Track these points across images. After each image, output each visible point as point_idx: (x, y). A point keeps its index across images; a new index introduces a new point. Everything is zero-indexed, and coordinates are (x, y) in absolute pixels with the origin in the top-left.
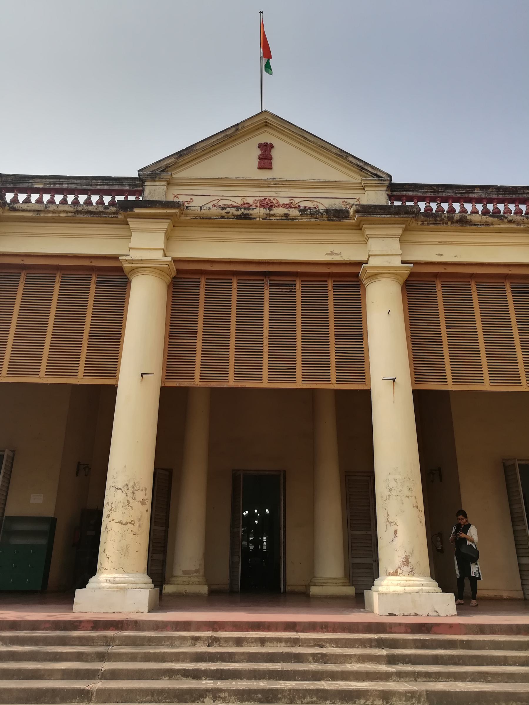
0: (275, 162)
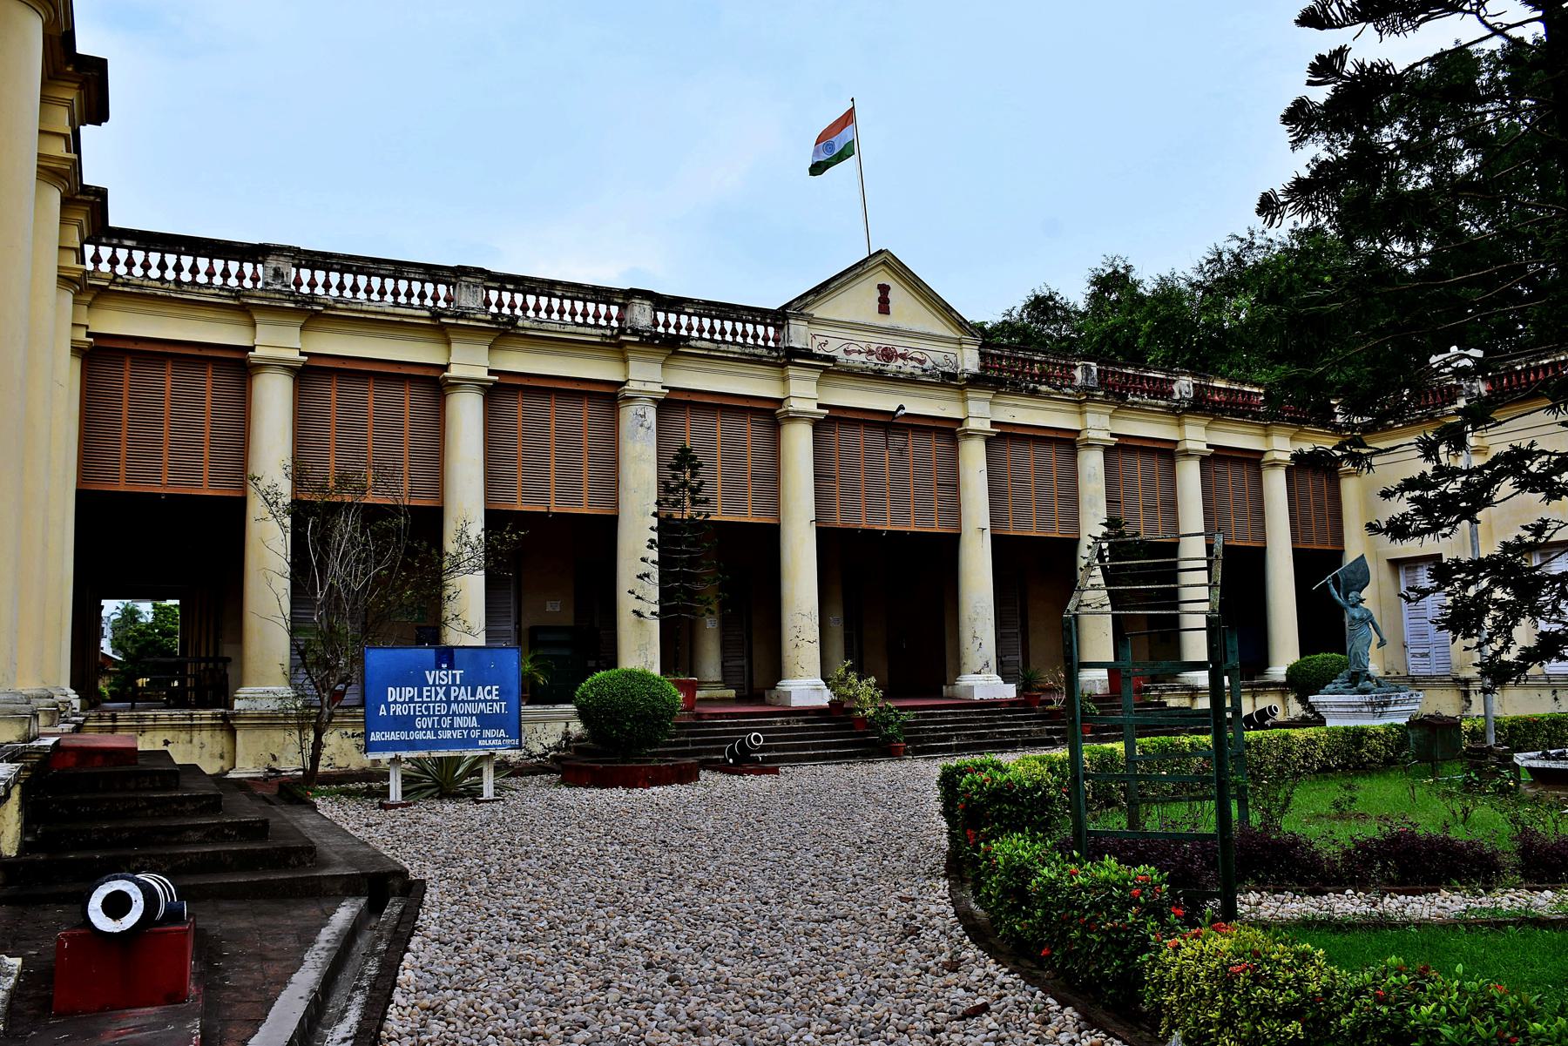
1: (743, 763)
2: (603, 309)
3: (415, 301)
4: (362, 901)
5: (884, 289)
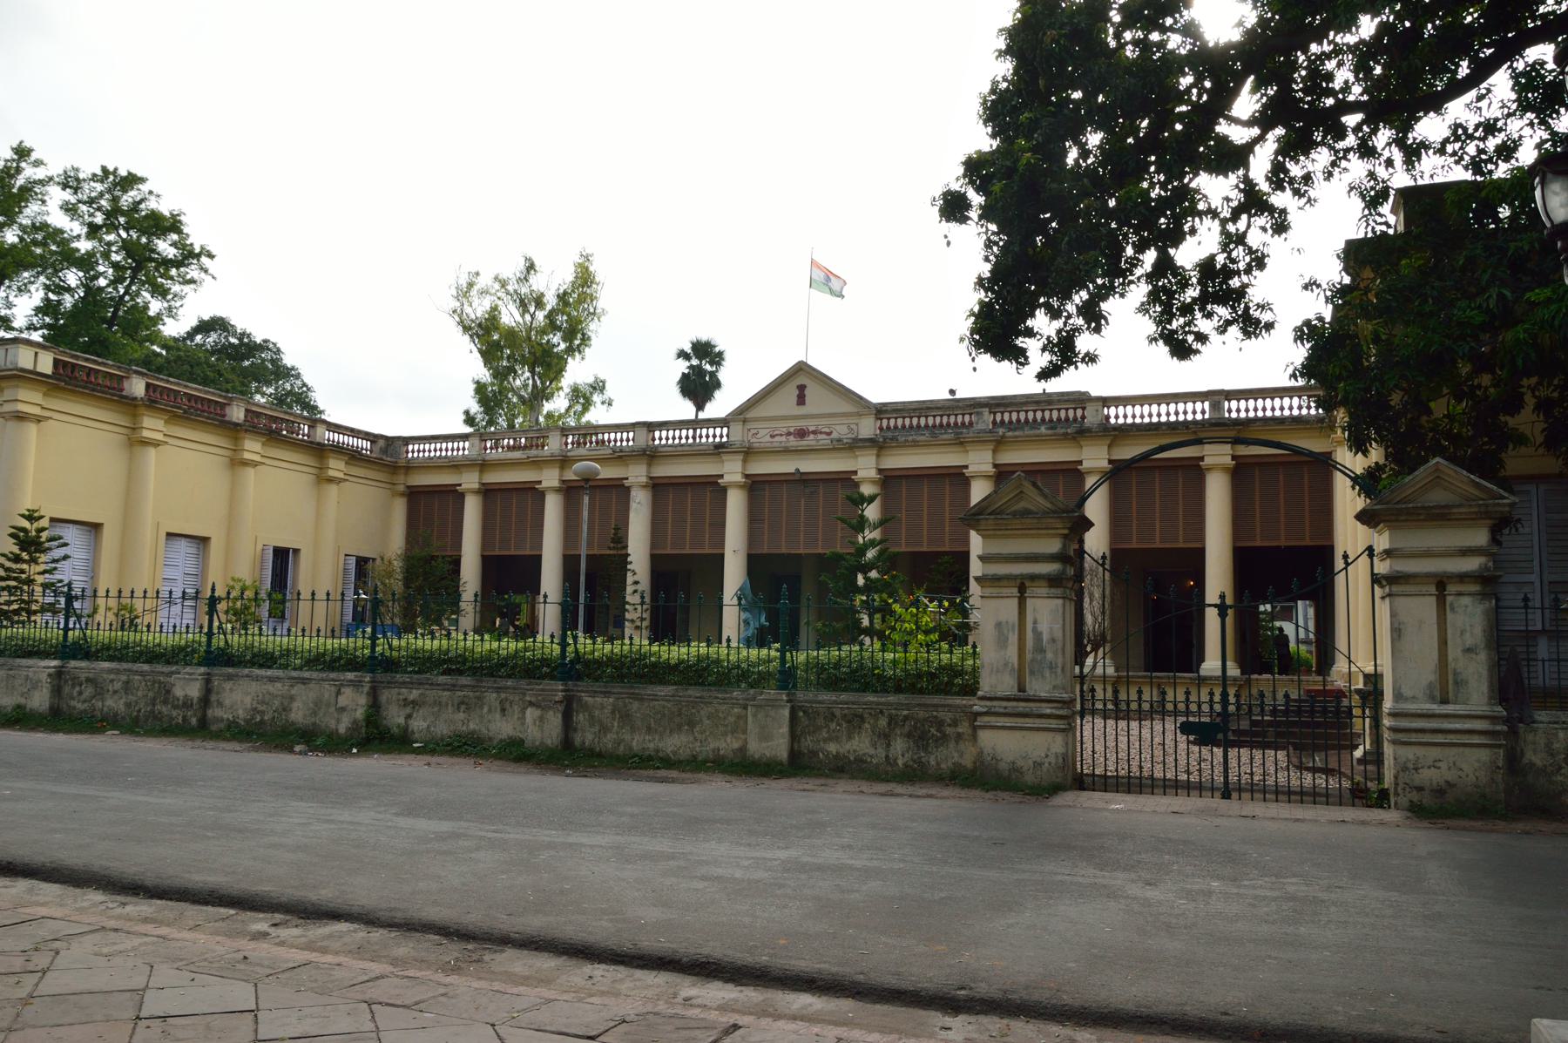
5: (802, 388)
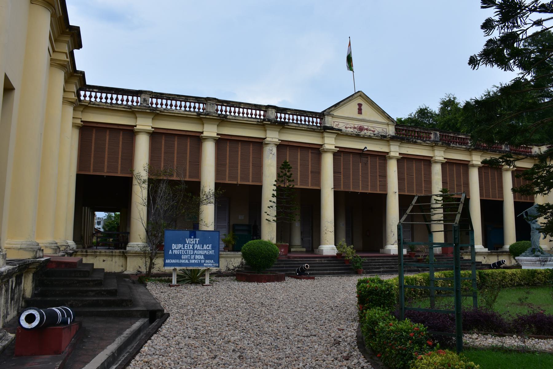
0: (363, 111)
1: (301, 274)
2: (258, 112)
3: (192, 109)
4: (146, 320)
5: (360, 105)
